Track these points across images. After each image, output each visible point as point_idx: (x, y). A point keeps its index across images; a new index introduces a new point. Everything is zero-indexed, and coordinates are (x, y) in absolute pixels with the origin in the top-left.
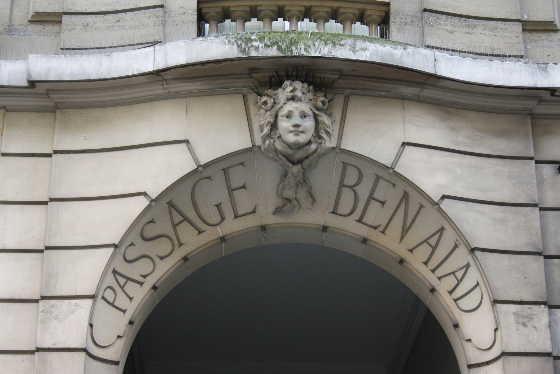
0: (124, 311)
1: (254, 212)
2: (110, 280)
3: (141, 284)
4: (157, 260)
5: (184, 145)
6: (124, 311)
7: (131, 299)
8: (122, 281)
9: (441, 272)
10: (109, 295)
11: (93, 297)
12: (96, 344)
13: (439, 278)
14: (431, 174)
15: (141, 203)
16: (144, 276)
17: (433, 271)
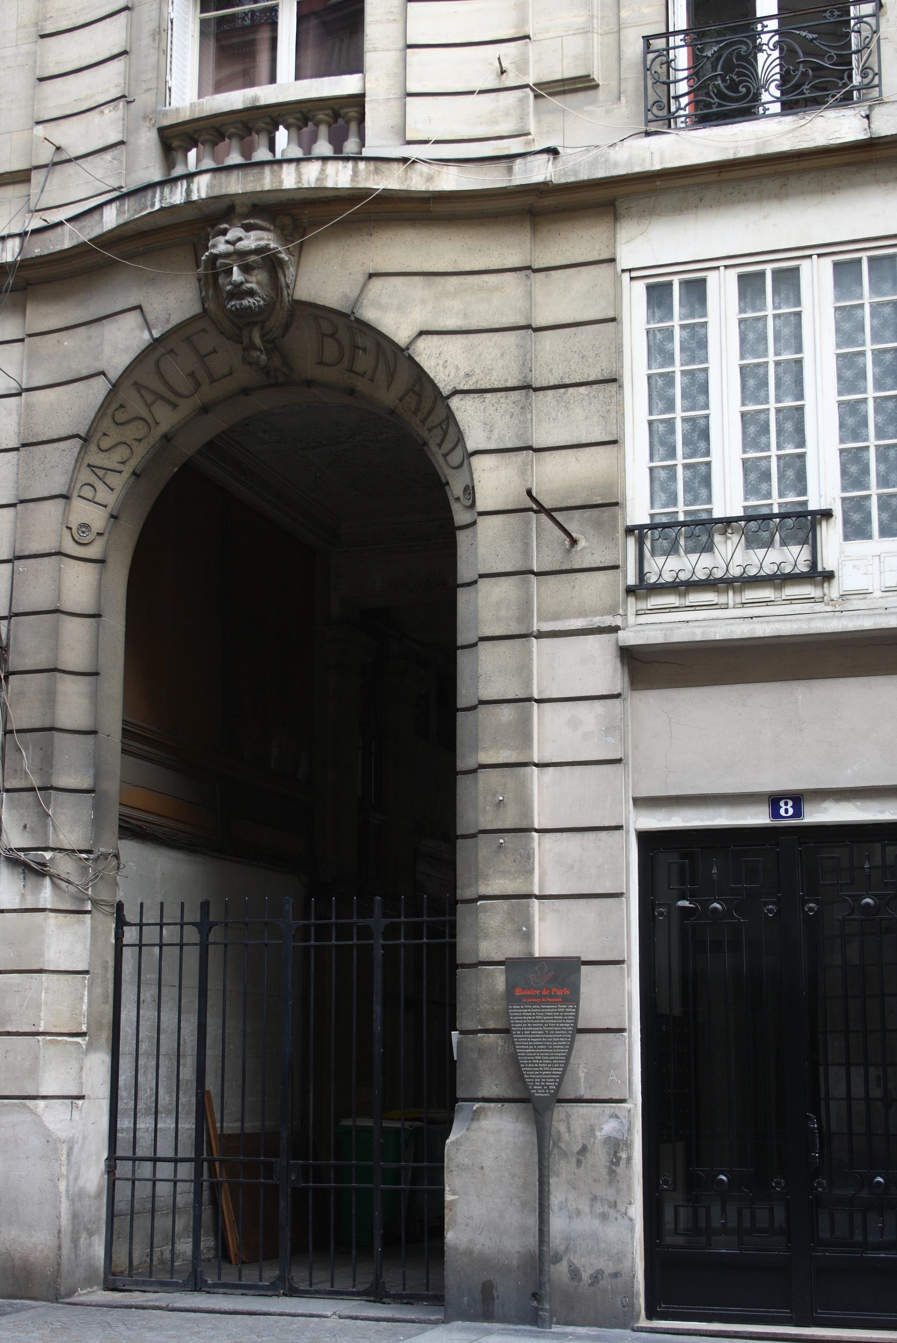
0: (105, 506)
1: (231, 373)
2: (86, 475)
3: (120, 472)
4: (136, 444)
5: (139, 311)
6: (105, 506)
7: (112, 490)
8: (101, 473)
9: (429, 424)
10: (87, 492)
11: (66, 497)
12: (340, 361)
13: (430, 430)
14: (397, 314)
15: (99, 389)
16: (123, 463)
17: (423, 422)
